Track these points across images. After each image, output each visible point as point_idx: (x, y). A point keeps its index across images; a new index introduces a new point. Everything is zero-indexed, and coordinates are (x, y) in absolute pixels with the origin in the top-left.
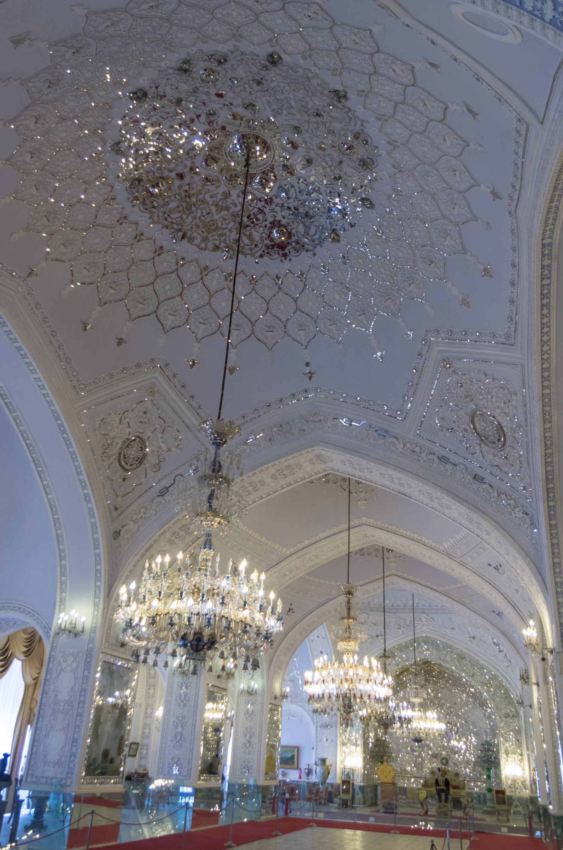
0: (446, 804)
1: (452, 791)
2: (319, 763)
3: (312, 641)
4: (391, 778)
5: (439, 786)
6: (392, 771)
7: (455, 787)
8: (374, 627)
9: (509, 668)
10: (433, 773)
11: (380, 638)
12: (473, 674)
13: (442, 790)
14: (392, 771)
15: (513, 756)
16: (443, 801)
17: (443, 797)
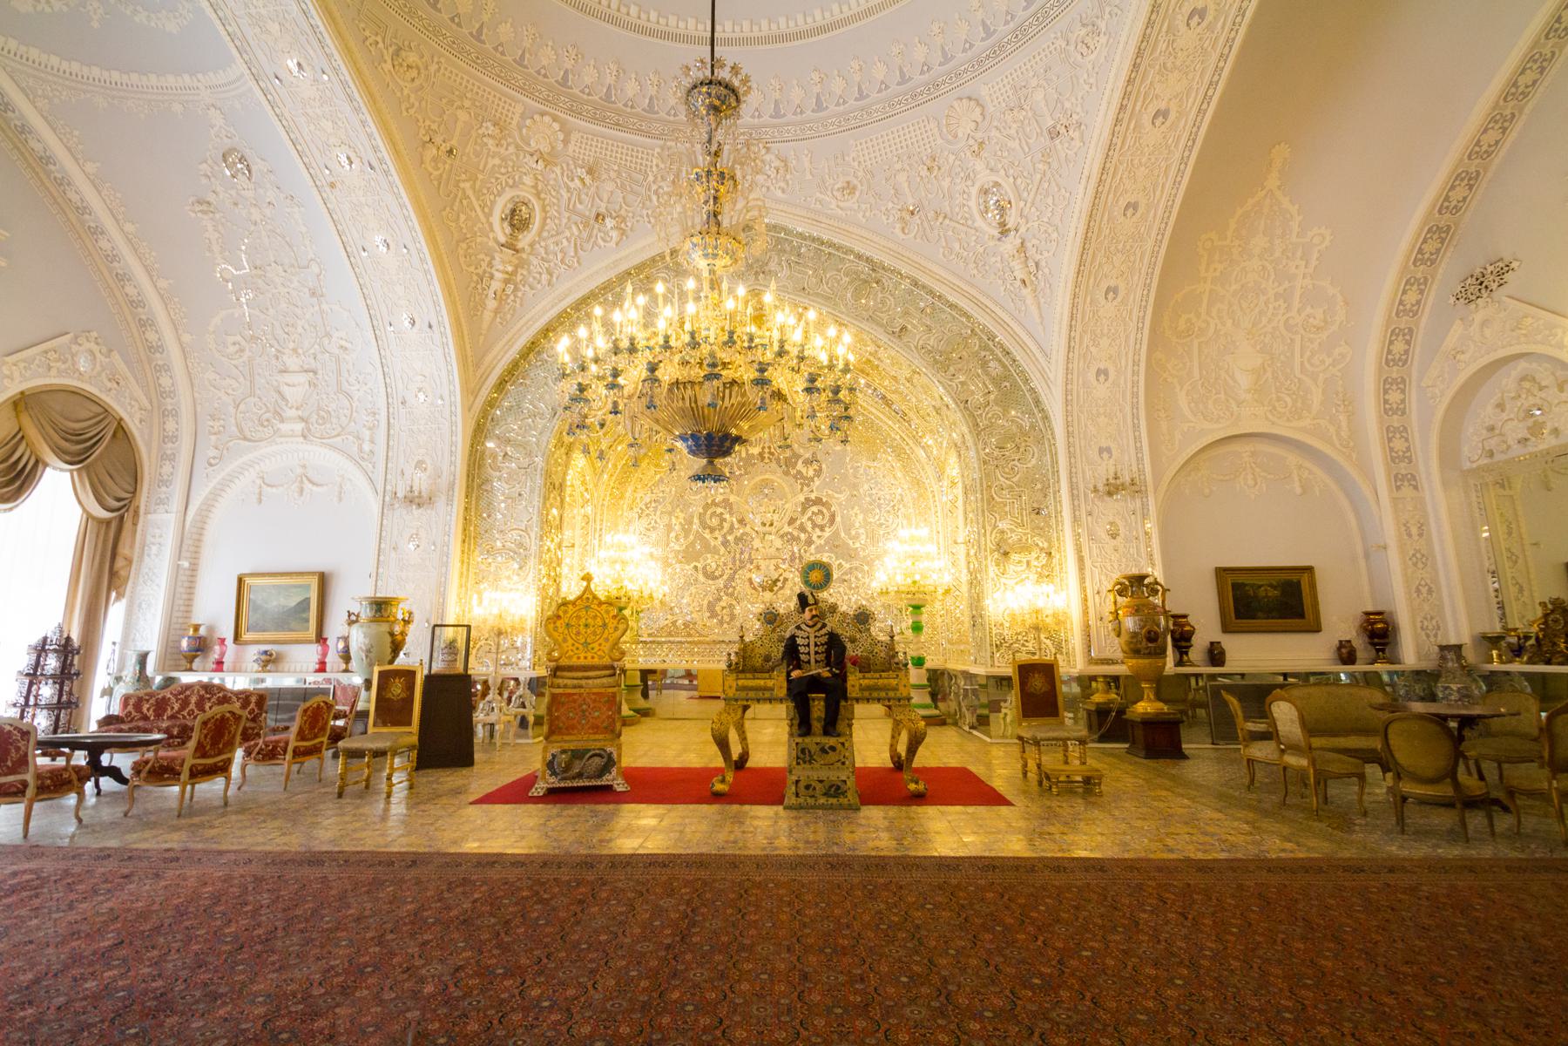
0: (832, 741)
1: (855, 681)
2: (366, 613)
3: (332, 185)
4: (606, 647)
5: (798, 667)
6: (611, 624)
7: (864, 666)
8: (588, 180)
9: (1026, 292)
10: (771, 618)
11: (609, 223)
12: (903, 329)
13: (815, 683)
14: (611, 624)
15: (1023, 557)
16: (817, 726)
17: (818, 707)
